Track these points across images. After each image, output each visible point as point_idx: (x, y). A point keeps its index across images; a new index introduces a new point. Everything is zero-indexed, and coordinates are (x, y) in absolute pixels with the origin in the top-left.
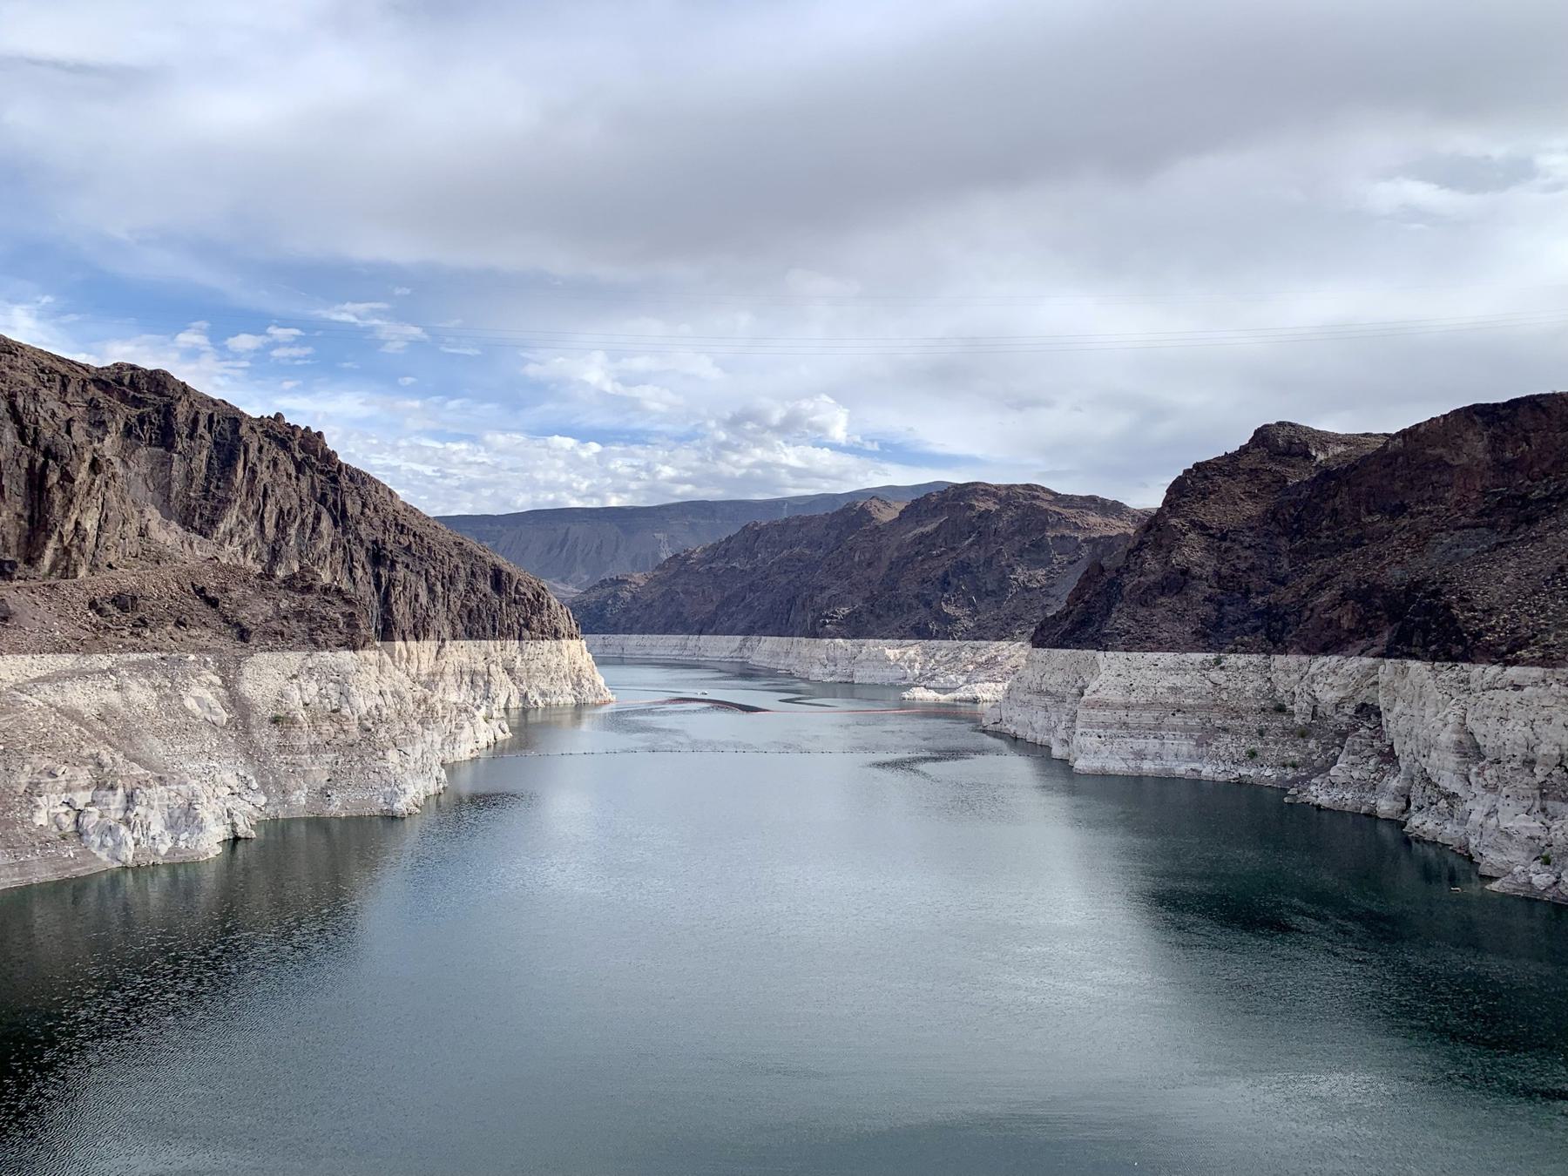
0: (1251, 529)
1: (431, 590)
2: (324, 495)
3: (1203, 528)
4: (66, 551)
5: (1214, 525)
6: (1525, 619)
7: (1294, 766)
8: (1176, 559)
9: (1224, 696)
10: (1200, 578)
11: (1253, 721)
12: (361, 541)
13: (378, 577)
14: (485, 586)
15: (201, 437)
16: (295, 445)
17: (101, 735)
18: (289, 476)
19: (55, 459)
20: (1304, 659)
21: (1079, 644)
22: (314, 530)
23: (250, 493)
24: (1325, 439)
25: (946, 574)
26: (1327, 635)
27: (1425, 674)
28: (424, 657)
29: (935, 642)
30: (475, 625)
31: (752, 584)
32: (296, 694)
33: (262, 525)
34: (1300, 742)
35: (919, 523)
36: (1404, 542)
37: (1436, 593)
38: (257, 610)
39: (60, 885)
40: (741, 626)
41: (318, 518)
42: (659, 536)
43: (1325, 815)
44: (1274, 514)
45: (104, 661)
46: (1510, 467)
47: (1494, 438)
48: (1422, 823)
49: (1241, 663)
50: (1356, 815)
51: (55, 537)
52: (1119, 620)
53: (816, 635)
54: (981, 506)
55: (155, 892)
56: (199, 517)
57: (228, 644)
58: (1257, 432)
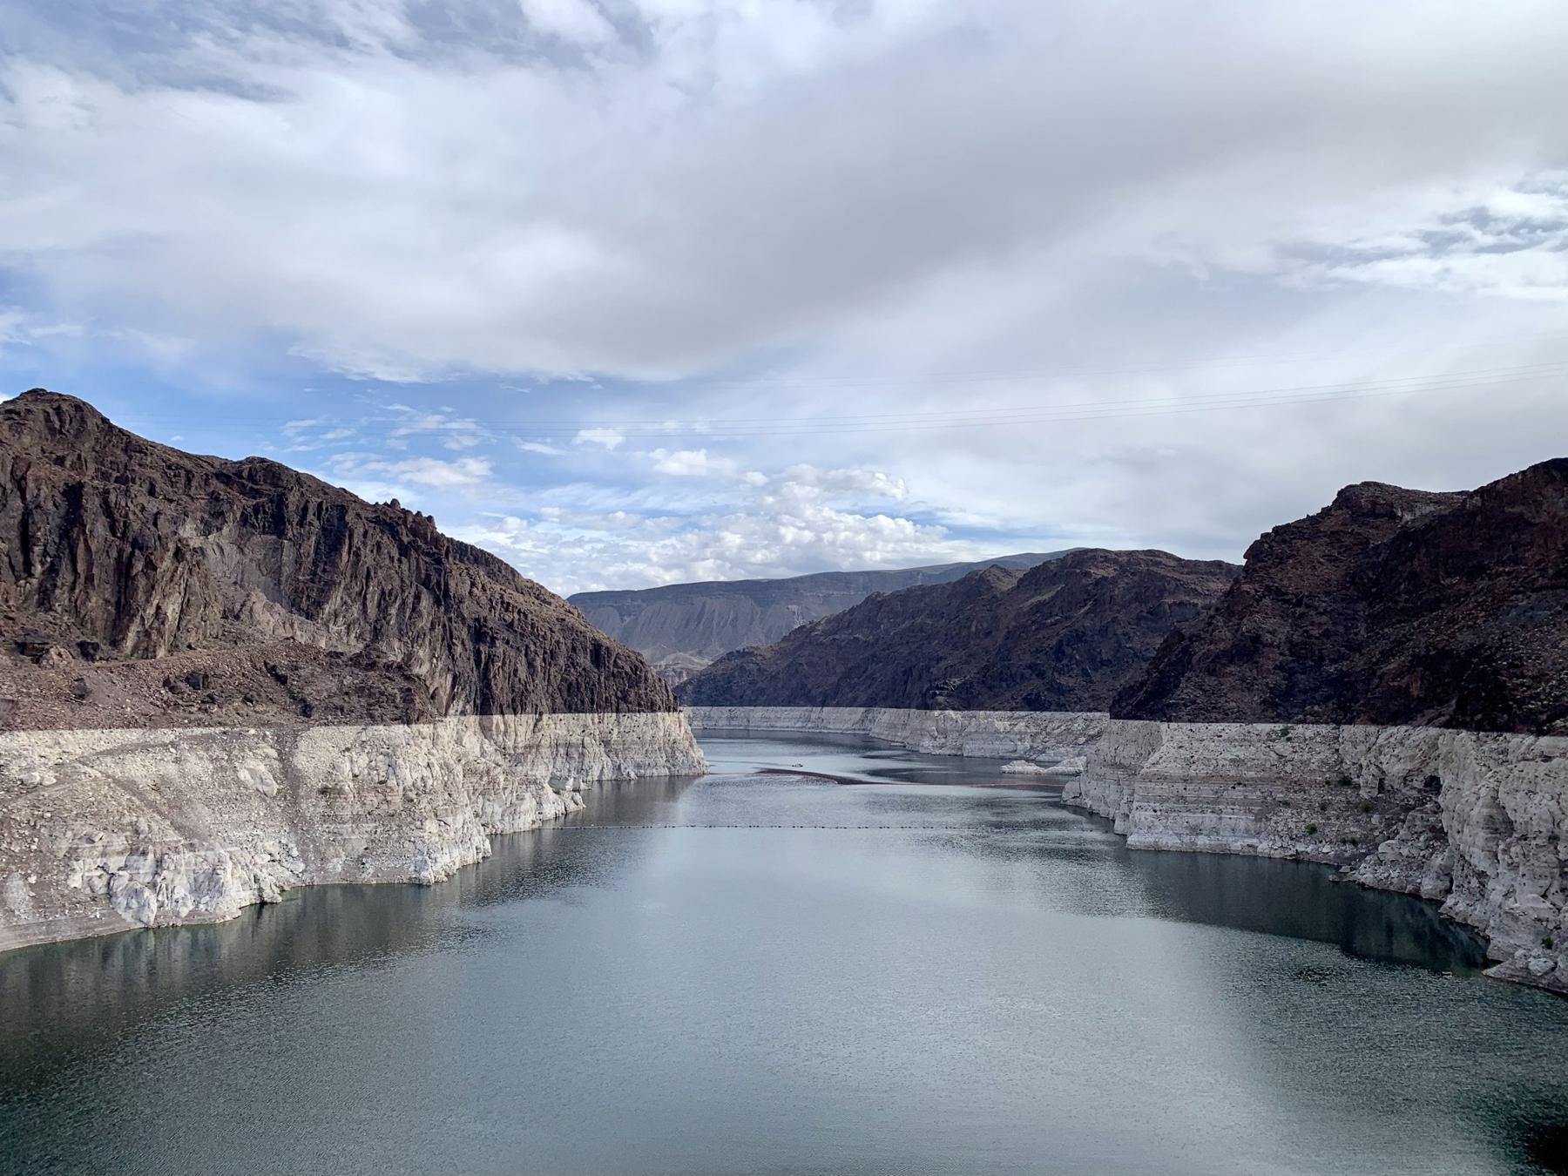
0: (1328, 594)
1: (531, 665)
2: (428, 576)
3: (1278, 594)
4: (147, 634)
7: (1354, 842)
9: (1288, 768)
10: (1271, 645)
11: (1315, 795)
12: (464, 618)
13: (478, 653)
14: (585, 660)
15: (311, 524)
16: (403, 530)
17: (152, 805)
18: (392, 559)
19: (141, 549)
20: (1372, 729)
22: (414, 610)
23: (354, 576)
24: (1411, 498)
25: (1060, 642)
28: (521, 730)
29: (1048, 714)
30: (574, 699)
31: (874, 656)
32: (347, 767)
33: (364, 605)
34: (1363, 817)
35: (1038, 592)
37: (1489, 660)
38: (322, 686)
39: (84, 943)
40: (863, 698)
41: (418, 598)
42: (794, 608)
43: (1370, 896)
44: (1353, 577)
45: (166, 735)
48: (1456, 904)
49: (1308, 734)
51: (137, 620)
52: (1186, 690)
54: (1098, 572)
55: (179, 951)
56: (305, 601)
57: (289, 719)
58: (1340, 493)
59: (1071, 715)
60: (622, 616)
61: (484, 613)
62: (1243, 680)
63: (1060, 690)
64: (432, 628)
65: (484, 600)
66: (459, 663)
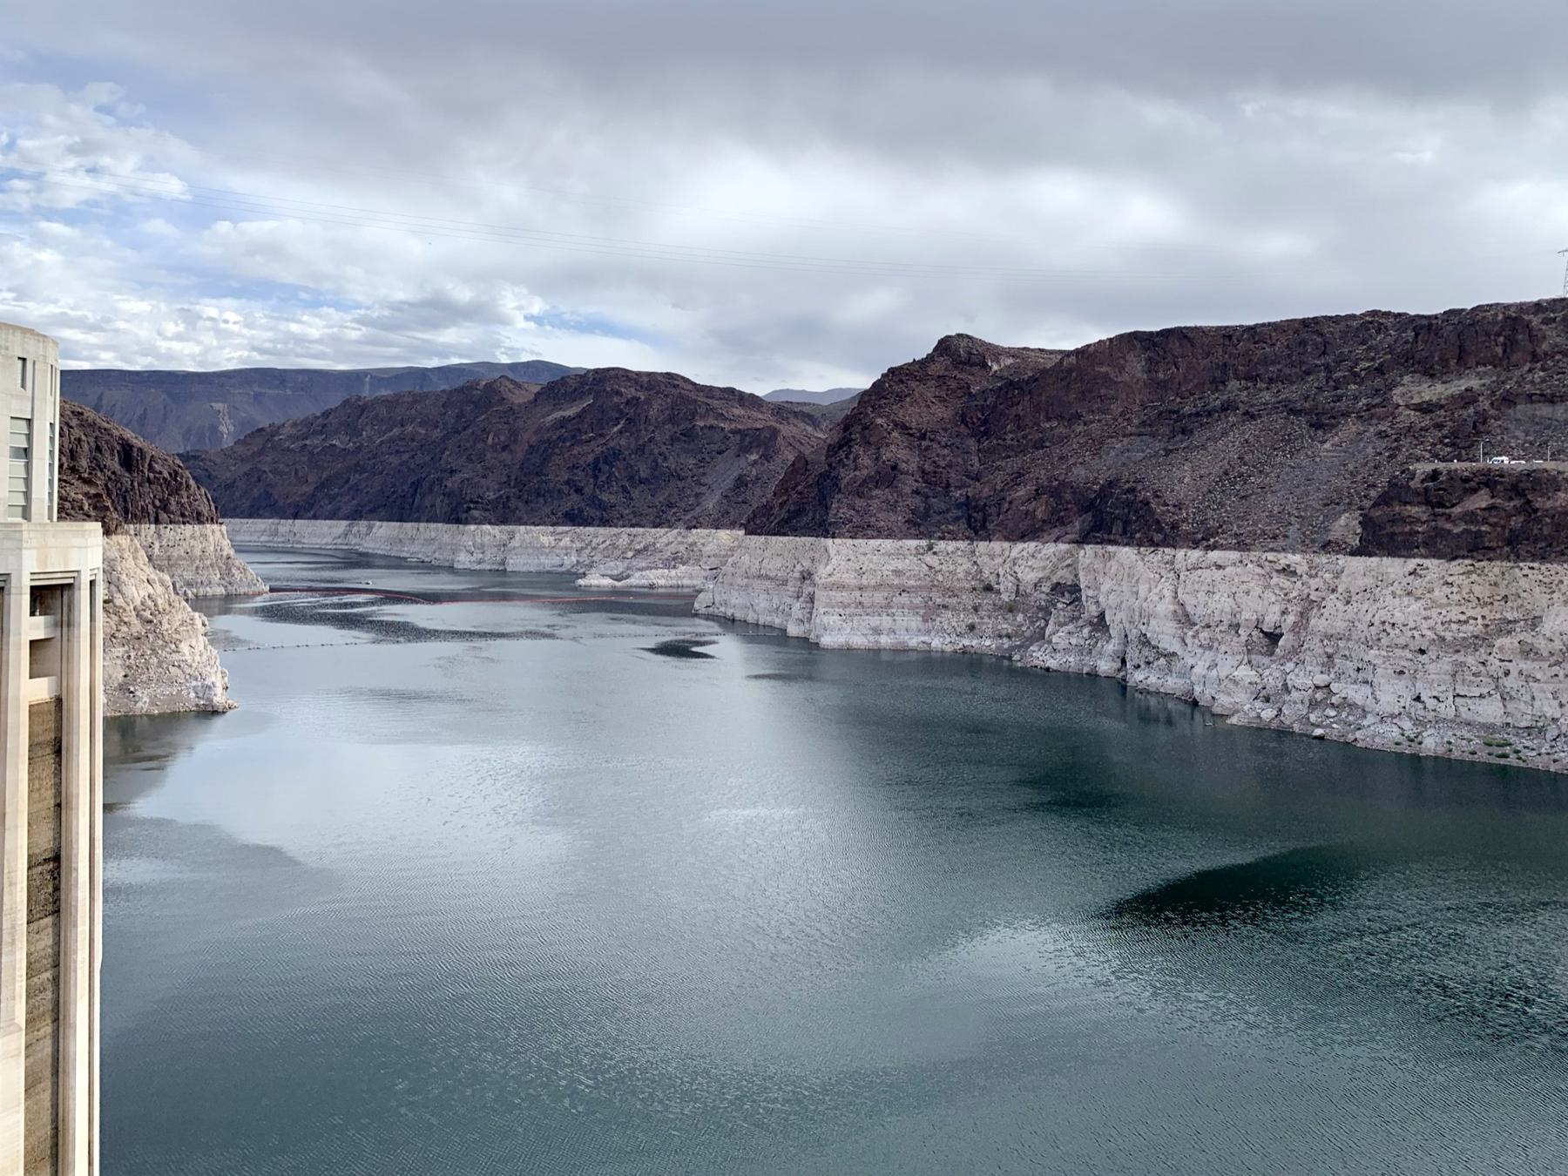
0: (945, 430)
3: (904, 428)
5: (914, 425)
6: (1210, 513)
7: (1009, 636)
8: (886, 455)
9: (940, 578)
11: (968, 599)
14: (114, 463)
20: (1006, 545)
21: (796, 532)
24: (997, 352)
25: (597, 460)
26: (1024, 525)
27: (1134, 557)
31: (357, 465)
36: (1082, 446)
37: (1132, 490)
46: (1163, 386)
47: (1149, 359)
50: (1079, 675)
52: (840, 508)
53: (458, 521)
54: (630, 392)
58: (941, 342)
59: (614, 530)
62: (887, 501)
63: (602, 506)
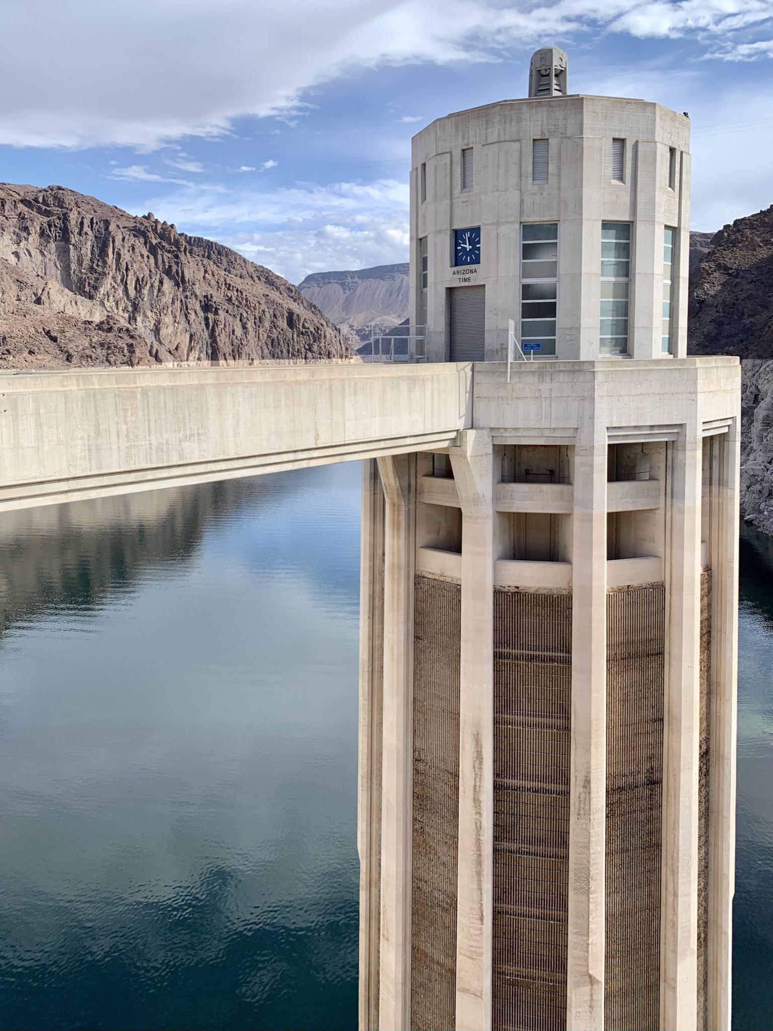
1: (244, 327)
2: (170, 267)
10: (712, 306)
12: (196, 296)
13: (206, 319)
14: (283, 323)
15: (86, 234)
16: (151, 235)
18: (142, 256)
20: (758, 362)
22: (159, 290)
23: (118, 268)
30: (277, 349)
33: (126, 290)
38: (79, 343)
41: (161, 282)
56: (84, 287)
60: (344, 289)
61: (211, 291)
64: (173, 303)
65: (213, 283)
66: (194, 326)
